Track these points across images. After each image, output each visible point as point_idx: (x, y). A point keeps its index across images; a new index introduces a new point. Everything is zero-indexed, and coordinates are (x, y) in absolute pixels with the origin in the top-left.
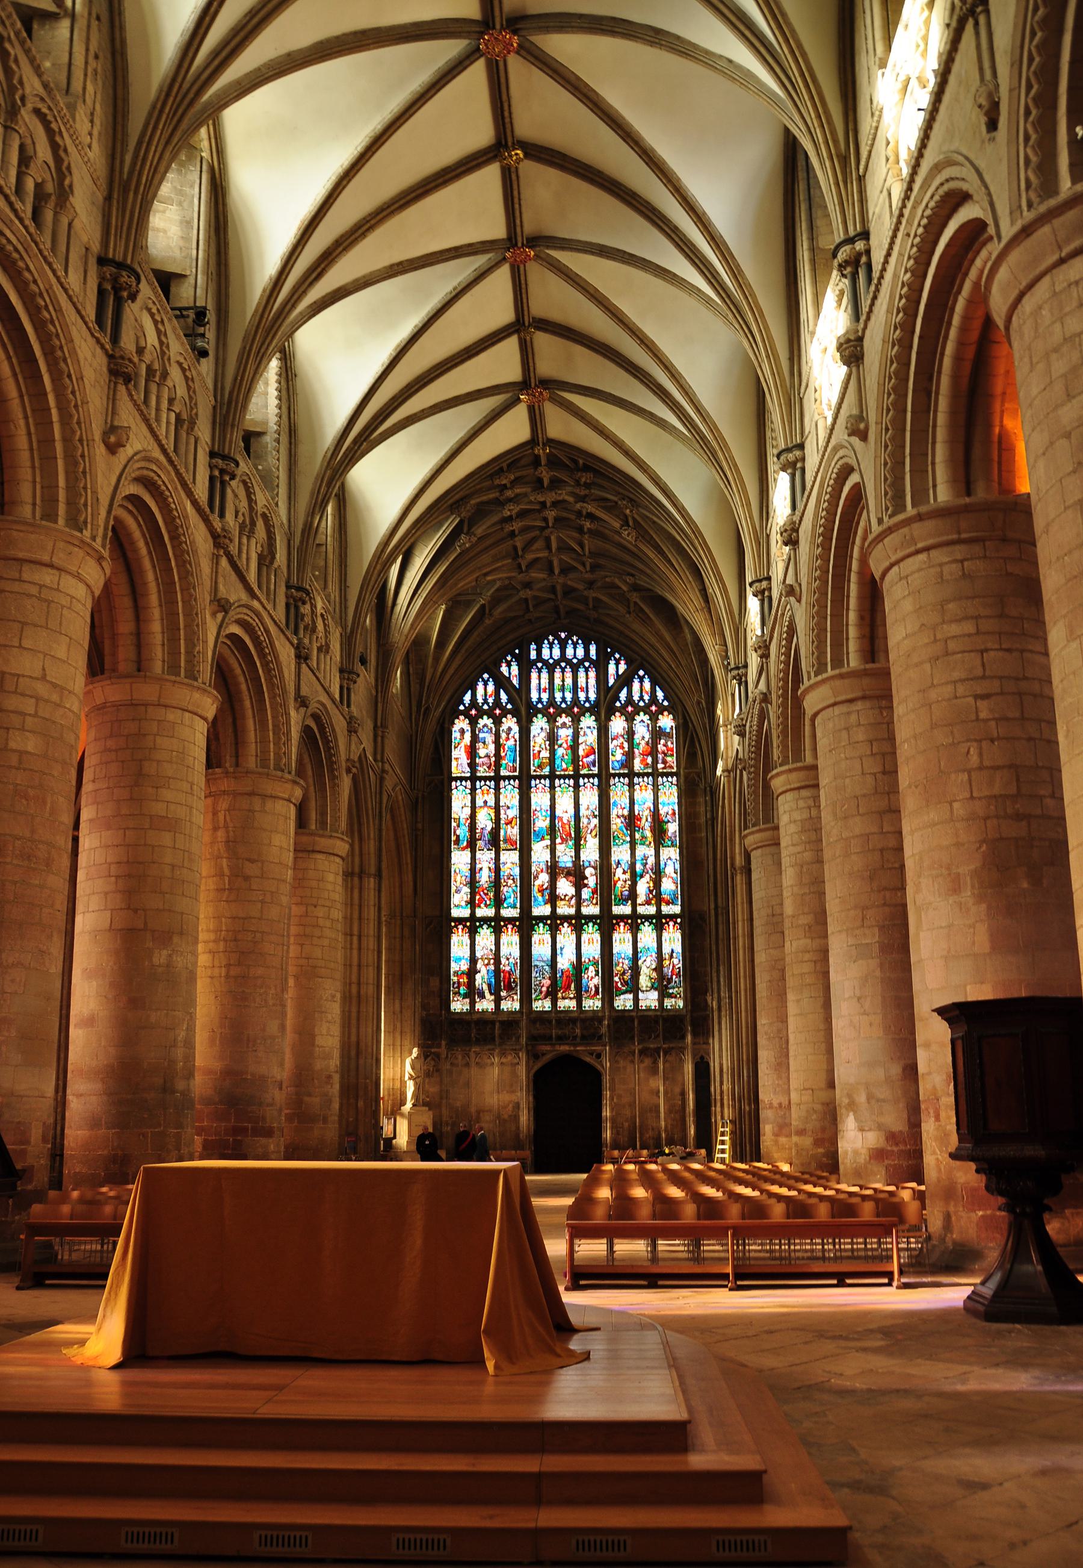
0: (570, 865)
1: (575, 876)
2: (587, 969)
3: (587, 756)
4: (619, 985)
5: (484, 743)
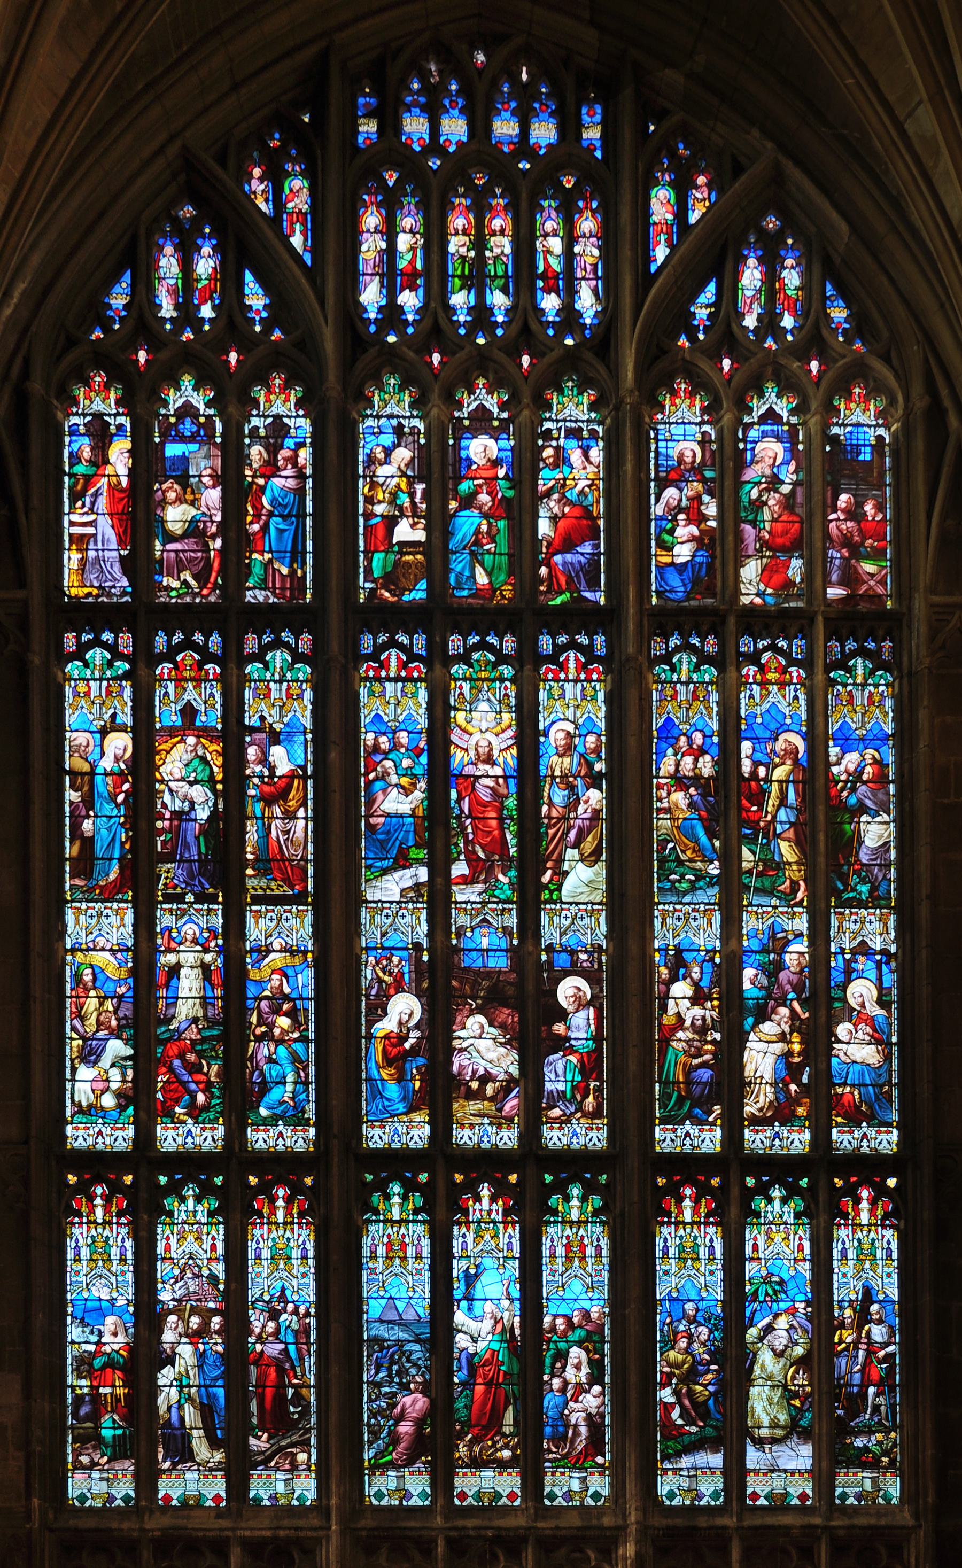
0: (499, 962)
1: (519, 1006)
2: (562, 1356)
3: (567, 544)
4: (675, 1414)
5: (183, 480)
